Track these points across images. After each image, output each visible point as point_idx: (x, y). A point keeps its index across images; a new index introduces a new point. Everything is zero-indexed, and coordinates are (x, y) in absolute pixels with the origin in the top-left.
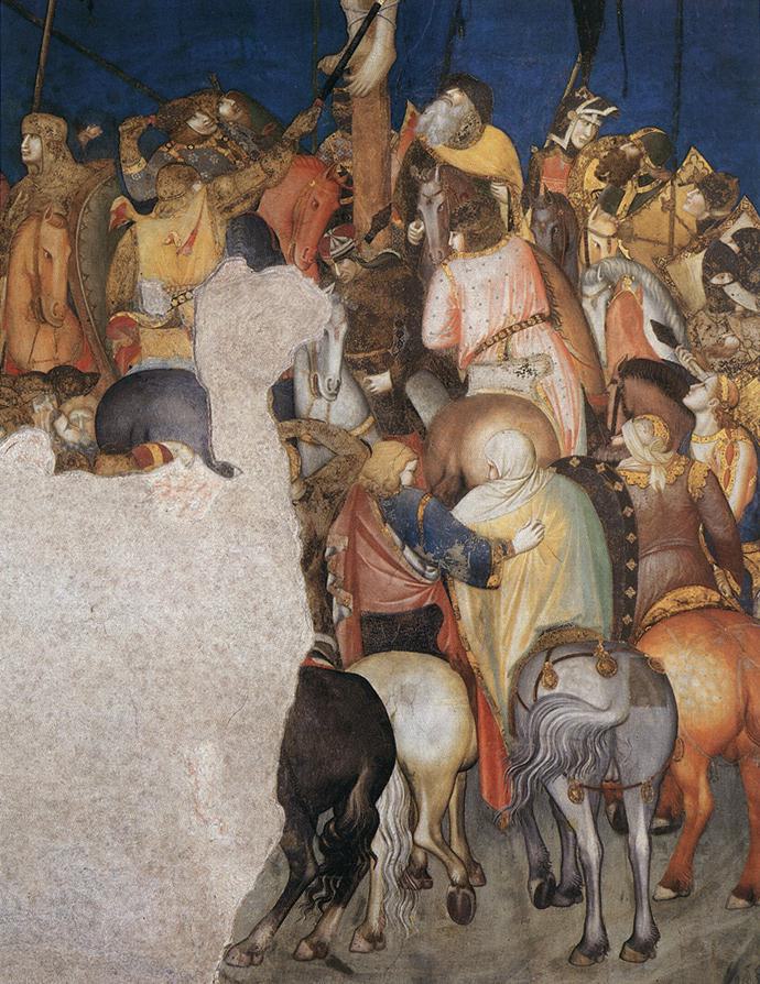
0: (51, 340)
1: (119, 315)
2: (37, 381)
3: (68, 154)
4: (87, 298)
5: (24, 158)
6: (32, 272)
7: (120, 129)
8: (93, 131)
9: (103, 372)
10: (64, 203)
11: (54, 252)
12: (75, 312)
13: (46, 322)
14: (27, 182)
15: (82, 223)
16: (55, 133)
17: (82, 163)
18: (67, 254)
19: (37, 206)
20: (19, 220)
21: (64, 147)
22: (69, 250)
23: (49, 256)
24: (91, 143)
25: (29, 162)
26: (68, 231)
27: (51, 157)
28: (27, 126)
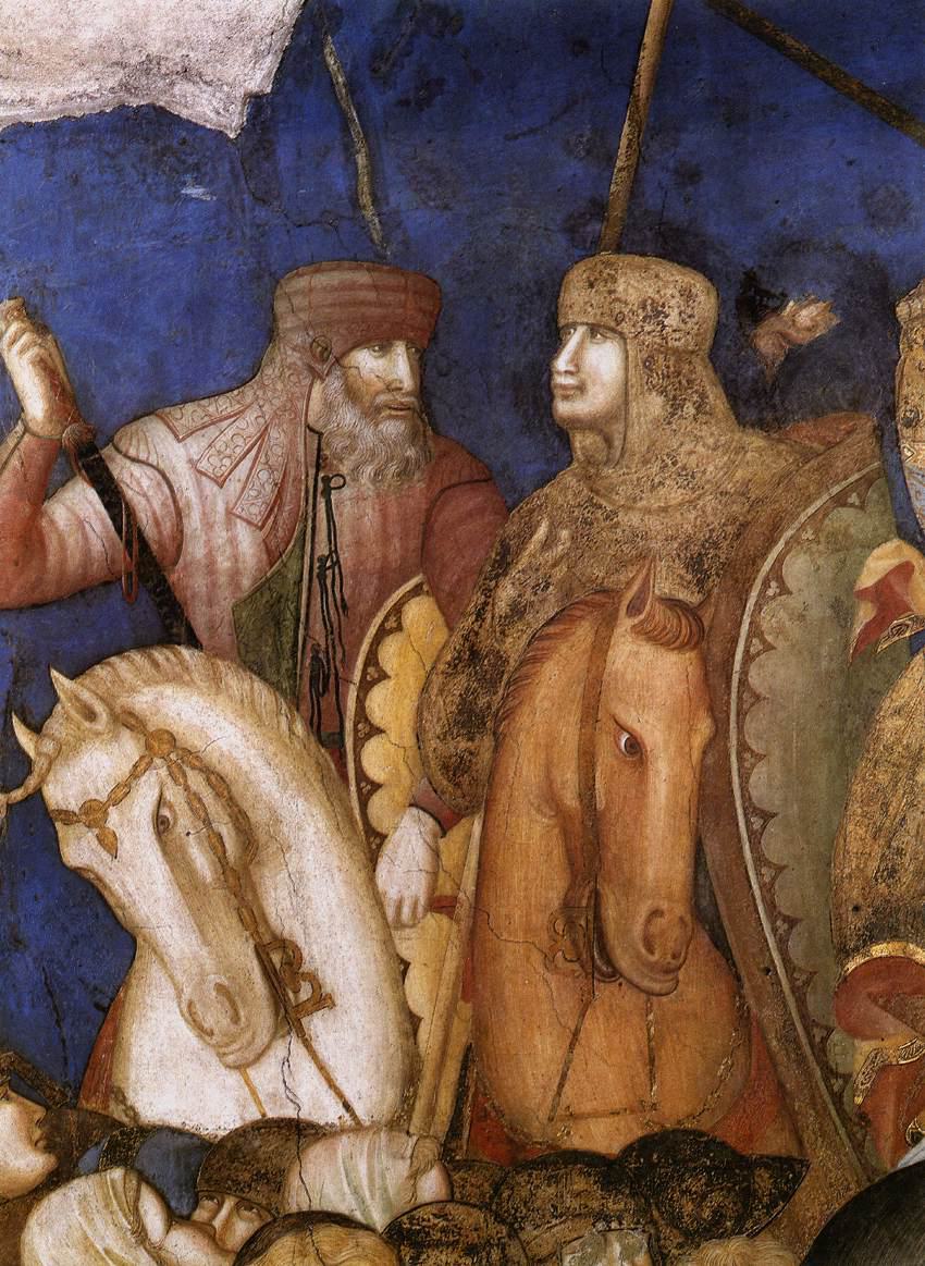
0: (633, 1040)
1: (880, 950)
2: (580, 1184)
3: (716, 399)
4: (768, 889)
5: (563, 408)
6: (570, 800)
7: (902, 310)
8: (806, 317)
9: (820, 1155)
10: (695, 564)
11: (654, 731)
12: (719, 942)
13: (614, 974)
14: (567, 488)
15: (756, 631)
16: (673, 320)
17: (761, 425)
18: (698, 741)
19: (599, 573)
20: (537, 619)
21: (703, 374)
22: (704, 727)
23: (635, 746)
24: (797, 359)
25: (577, 423)
26: (704, 660)
27: (656, 404)
28: (577, 297)
